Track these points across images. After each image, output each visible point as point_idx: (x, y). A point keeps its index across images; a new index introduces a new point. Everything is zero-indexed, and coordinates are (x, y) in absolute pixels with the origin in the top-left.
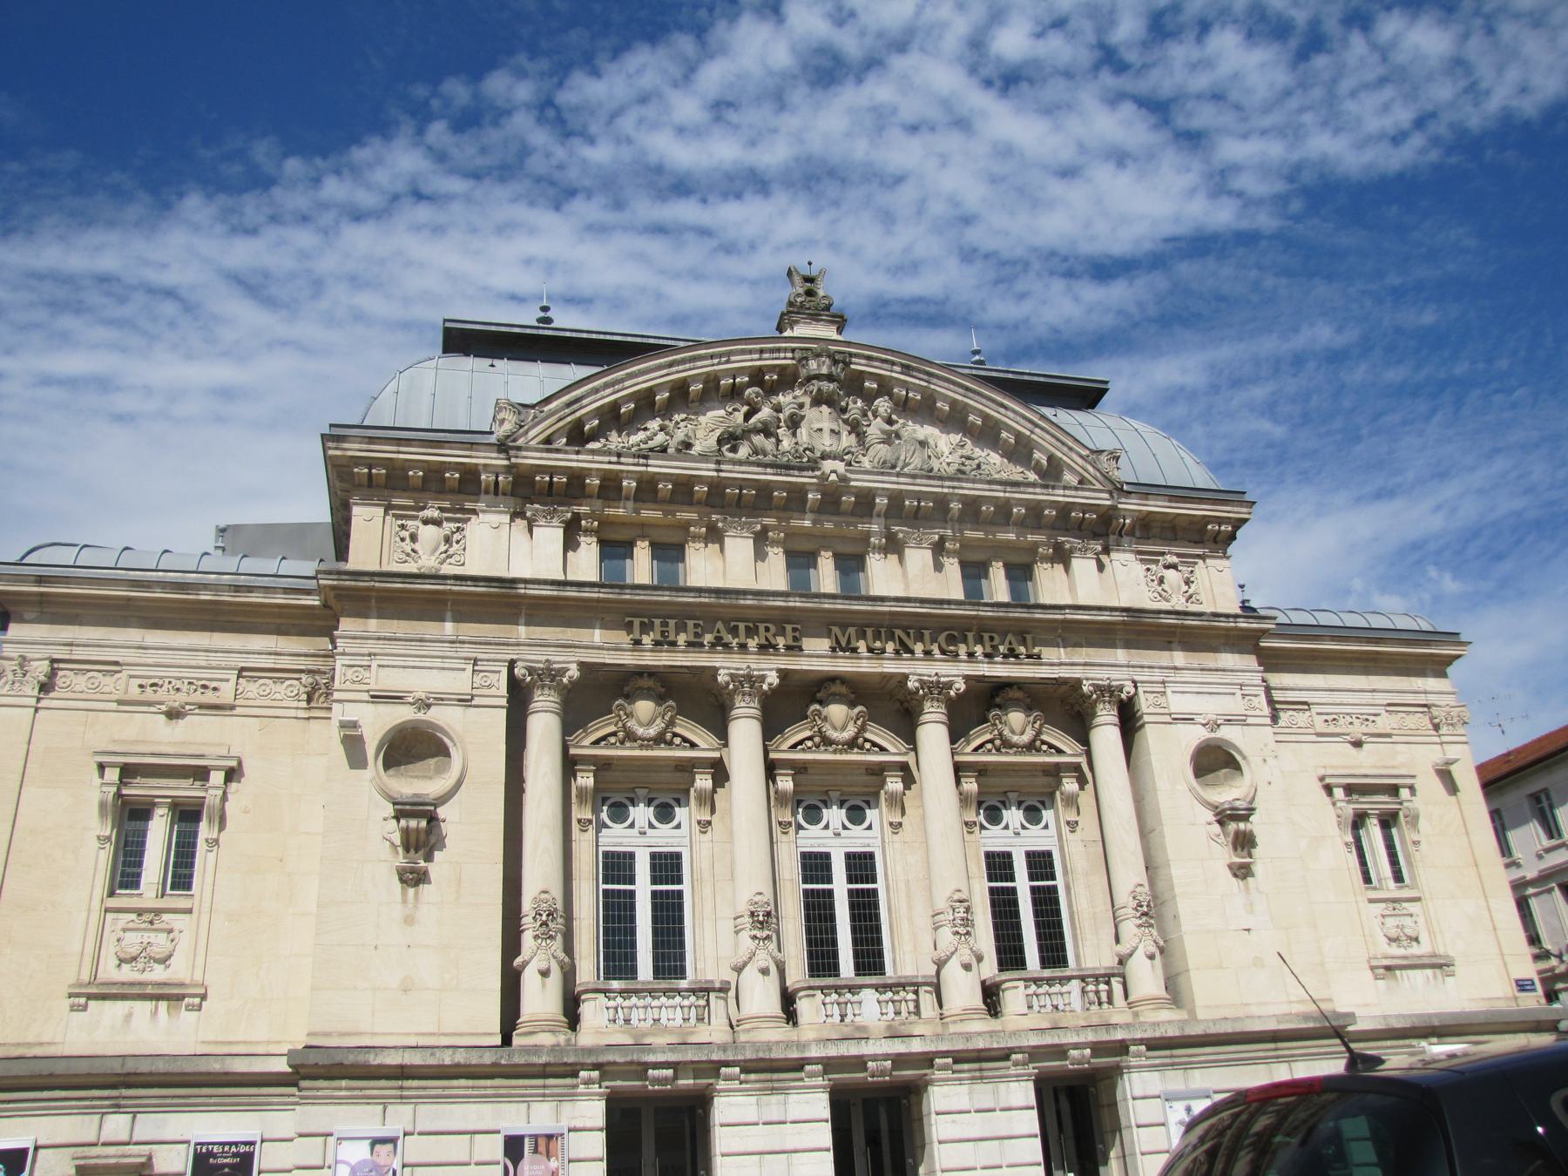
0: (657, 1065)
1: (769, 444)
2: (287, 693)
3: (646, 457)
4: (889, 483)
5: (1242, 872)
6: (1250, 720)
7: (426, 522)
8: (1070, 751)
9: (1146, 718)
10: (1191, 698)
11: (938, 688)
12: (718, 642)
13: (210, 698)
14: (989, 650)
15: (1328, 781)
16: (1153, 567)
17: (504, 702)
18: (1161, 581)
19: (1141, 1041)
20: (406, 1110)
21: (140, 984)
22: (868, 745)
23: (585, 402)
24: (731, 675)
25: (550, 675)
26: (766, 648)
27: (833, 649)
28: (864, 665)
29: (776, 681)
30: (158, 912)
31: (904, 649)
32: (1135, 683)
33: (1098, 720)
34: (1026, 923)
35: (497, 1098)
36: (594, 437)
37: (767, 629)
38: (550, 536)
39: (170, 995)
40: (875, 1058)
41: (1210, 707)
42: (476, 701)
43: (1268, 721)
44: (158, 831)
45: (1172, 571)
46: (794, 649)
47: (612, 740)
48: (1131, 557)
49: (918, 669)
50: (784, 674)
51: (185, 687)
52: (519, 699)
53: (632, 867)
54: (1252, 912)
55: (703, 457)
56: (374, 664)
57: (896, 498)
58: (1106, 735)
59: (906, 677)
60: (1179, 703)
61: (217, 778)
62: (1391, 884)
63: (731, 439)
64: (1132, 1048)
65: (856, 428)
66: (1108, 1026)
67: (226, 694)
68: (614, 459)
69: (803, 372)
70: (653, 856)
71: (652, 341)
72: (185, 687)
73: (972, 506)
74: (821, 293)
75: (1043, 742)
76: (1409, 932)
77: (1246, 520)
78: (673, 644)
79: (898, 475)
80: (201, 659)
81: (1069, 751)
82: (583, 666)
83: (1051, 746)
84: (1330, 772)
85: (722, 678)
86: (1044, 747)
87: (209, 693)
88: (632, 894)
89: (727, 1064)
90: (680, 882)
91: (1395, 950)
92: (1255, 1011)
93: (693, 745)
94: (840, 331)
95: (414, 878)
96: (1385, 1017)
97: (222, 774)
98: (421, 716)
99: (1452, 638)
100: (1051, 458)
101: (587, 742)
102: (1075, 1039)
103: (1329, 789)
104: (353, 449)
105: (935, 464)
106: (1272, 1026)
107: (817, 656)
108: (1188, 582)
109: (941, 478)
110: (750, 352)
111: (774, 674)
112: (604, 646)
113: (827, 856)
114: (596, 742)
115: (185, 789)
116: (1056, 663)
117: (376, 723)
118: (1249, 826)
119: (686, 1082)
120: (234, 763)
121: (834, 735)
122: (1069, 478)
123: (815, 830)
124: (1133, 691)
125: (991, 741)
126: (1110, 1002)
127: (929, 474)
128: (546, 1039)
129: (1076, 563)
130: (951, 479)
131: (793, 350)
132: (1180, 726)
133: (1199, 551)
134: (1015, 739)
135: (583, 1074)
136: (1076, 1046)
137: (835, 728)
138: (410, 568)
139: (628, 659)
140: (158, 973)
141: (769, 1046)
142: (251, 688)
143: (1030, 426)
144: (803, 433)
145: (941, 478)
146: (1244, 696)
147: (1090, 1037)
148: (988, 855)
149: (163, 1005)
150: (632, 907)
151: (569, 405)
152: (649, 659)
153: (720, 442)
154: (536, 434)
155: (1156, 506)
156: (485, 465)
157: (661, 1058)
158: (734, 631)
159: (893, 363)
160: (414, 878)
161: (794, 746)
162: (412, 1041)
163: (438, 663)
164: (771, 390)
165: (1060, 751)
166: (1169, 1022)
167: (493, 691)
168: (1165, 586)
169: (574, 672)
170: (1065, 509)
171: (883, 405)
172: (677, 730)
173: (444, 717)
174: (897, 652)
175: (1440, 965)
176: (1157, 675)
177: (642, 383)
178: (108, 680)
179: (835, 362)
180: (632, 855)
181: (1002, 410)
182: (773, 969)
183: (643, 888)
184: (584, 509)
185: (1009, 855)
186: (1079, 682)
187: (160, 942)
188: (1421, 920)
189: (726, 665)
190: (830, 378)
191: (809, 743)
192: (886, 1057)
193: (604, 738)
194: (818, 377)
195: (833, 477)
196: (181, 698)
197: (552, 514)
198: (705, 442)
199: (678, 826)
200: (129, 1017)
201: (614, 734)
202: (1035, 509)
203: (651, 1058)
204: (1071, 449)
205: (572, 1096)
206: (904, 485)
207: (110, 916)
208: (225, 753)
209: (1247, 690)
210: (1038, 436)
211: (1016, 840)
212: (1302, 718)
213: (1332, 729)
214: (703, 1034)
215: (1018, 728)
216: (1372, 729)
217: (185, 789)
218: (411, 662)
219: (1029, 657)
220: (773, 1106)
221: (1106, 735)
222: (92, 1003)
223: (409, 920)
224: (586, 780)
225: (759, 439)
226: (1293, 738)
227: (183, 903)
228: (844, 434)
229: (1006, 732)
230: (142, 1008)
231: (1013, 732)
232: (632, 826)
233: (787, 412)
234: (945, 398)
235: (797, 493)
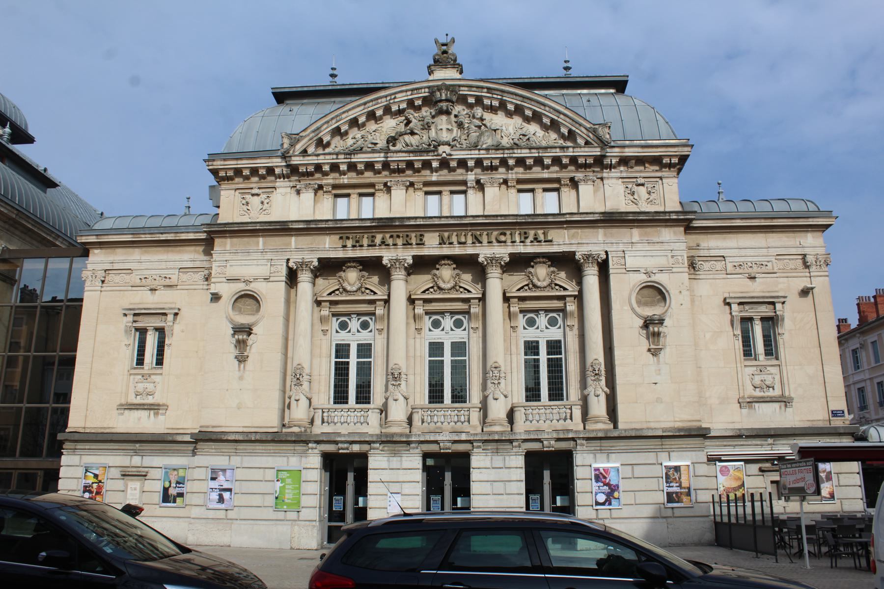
0: (342, 442)
1: (414, 140)
2: (199, 276)
3: (350, 154)
4: (475, 154)
5: (655, 352)
6: (674, 270)
7: (253, 195)
8: (572, 289)
9: (611, 271)
10: (639, 257)
11: (493, 260)
12: (383, 242)
13: (168, 282)
14: (523, 239)
15: (728, 301)
16: (630, 186)
17: (284, 279)
18: (633, 194)
19: (583, 438)
20: (239, 458)
21: (144, 405)
22: (461, 290)
23: (322, 129)
24: (390, 260)
25: (303, 264)
26: (407, 244)
27: (440, 244)
28: (457, 251)
29: (411, 262)
30: (150, 375)
31: (477, 240)
32: (606, 252)
33: (586, 273)
34: (547, 377)
35: (274, 453)
36: (328, 144)
37: (407, 236)
38: (308, 196)
39: (155, 408)
40: (443, 441)
41: (650, 263)
42: (271, 279)
43: (687, 270)
44: (151, 341)
45: (641, 187)
46: (421, 244)
47: (337, 292)
48: (614, 181)
49: (484, 252)
50: (414, 257)
51: (157, 278)
52: (292, 277)
53: (348, 351)
54: (660, 374)
55: (381, 151)
56: (228, 265)
57: (479, 162)
58: (591, 280)
59: (478, 255)
60: (631, 262)
61: (170, 317)
62: (762, 357)
63: (392, 140)
64: (578, 441)
65: (460, 125)
66: (568, 431)
67: (174, 280)
68: (335, 157)
69: (434, 99)
70: (359, 345)
71: (372, 86)
72: (157, 278)
73: (520, 162)
74: (450, 52)
75: (556, 285)
76: (767, 383)
77: (688, 156)
78: (361, 246)
79: (479, 150)
80: (163, 265)
81: (570, 289)
82: (320, 260)
83: (561, 286)
84: (732, 295)
85: (385, 261)
86: (557, 287)
87: (168, 280)
88: (348, 363)
89: (374, 442)
90: (370, 357)
91: (758, 393)
92: (653, 425)
93: (375, 293)
94: (461, 73)
95: (242, 359)
96: (740, 430)
97: (172, 316)
98: (247, 288)
99: (828, 214)
100: (570, 131)
101: (325, 294)
102: (546, 436)
103: (729, 304)
104: (218, 164)
105: (505, 142)
106: (660, 433)
107: (432, 246)
108: (649, 193)
109: (503, 149)
110: (406, 91)
111: (410, 258)
112: (329, 247)
113: (443, 343)
114: (330, 294)
115: (158, 322)
116: (562, 241)
117: (228, 291)
118: (661, 329)
119: (356, 448)
120: (176, 311)
121: (442, 285)
122: (581, 141)
123: (437, 331)
124: (605, 257)
125: (527, 285)
126: (571, 419)
127: (498, 147)
128: (296, 430)
129: (582, 187)
130: (508, 149)
131: (429, 87)
132: (631, 275)
133: (659, 174)
134: (539, 284)
135: (310, 445)
136: (547, 439)
137: (444, 282)
138: (246, 219)
139: (340, 254)
140: (150, 400)
141: (393, 435)
142: (184, 277)
143: (557, 114)
144: (433, 133)
145: (503, 149)
146: (672, 257)
147: (555, 435)
148: (525, 342)
149: (152, 412)
150: (348, 369)
151: (314, 131)
152: (350, 254)
153: (388, 142)
154: (299, 147)
155: (629, 152)
156: (277, 166)
157: (343, 439)
158: (391, 237)
159: (482, 88)
160: (242, 359)
161: (424, 292)
162: (241, 430)
163: (255, 262)
164: (418, 109)
165: (565, 289)
166: (600, 430)
167: (280, 274)
168: (636, 197)
169: (316, 263)
170: (574, 160)
171: (479, 111)
172: (368, 286)
173: (258, 287)
174: (473, 243)
175: (785, 401)
176: (621, 247)
177: (352, 115)
178: (127, 277)
179: (452, 91)
180: (349, 345)
181: (542, 107)
182: (401, 399)
183: (353, 360)
184: (324, 182)
185: (537, 342)
186: (574, 253)
187: (150, 387)
188: (777, 378)
189: (387, 256)
190: (447, 100)
191: (432, 290)
192: (449, 441)
193: (333, 292)
194: (441, 101)
195: (444, 155)
196: (157, 283)
197: (307, 186)
198: (382, 144)
199: (371, 331)
200: (139, 419)
201: (338, 290)
202: (557, 161)
203: (339, 439)
204: (580, 125)
205: (304, 454)
206: (483, 154)
207: (132, 377)
208: (173, 306)
209: (674, 253)
210: (561, 119)
211: (541, 335)
212: (719, 265)
213: (738, 270)
214: (364, 429)
215: (541, 278)
216: (764, 269)
217: (158, 322)
218: (244, 262)
219: (545, 241)
220: (395, 462)
221: (591, 280)
222: (126, 412)
223: (241, 378)
224: (325, 312)
225: (407, 138)
226: (711, 276)
227: (159, 371)
228: (455, 129)
229: (535, 281)
230: (144, 414)
231: (539, 280)
232: (349, 331)
233: (426, 121)
234: (512, 103)
235: (427, 165)
